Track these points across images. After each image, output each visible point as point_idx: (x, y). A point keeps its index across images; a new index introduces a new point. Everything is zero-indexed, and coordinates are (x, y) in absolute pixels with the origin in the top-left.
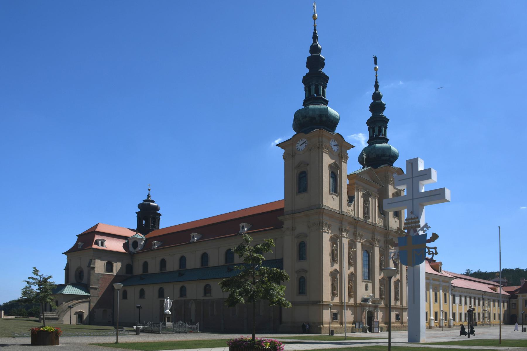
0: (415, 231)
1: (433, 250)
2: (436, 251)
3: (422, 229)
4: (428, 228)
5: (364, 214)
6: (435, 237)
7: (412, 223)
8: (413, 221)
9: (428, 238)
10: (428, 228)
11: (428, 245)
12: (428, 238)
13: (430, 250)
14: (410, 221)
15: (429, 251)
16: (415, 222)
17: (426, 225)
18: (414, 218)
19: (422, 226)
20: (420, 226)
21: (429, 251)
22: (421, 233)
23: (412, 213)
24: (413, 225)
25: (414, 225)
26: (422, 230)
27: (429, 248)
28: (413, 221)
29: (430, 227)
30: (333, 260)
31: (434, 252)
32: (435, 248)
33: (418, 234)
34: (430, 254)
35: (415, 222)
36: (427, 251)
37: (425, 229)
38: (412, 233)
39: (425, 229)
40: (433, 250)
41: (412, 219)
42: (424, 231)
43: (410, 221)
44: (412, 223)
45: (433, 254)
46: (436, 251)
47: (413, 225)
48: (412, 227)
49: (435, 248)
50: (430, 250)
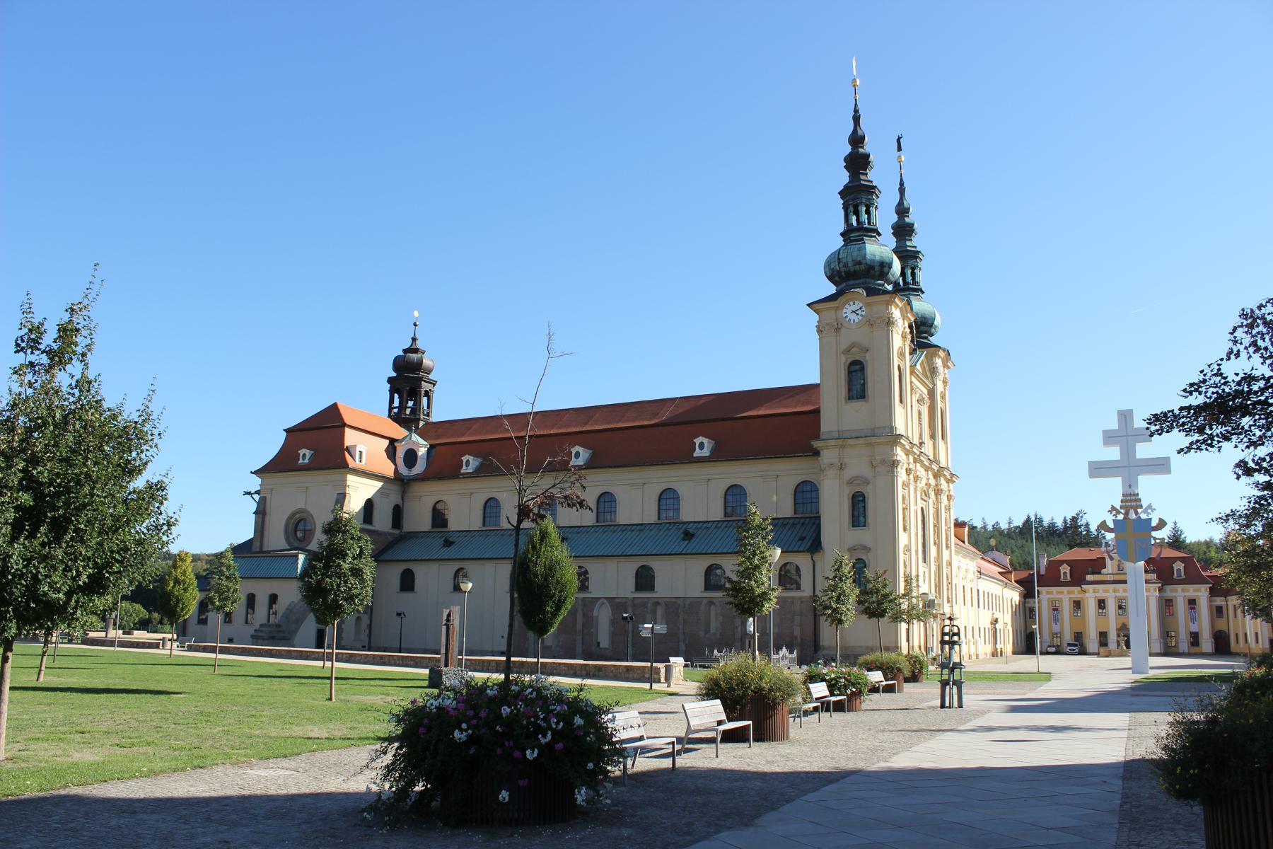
0: (1137, 513)
3: (1145, 511)
4: (1153, 510)
9: (1154, 524)
10: (1153, 510)
11: (1154, 534)
12: (1154, 524)
17: (1150, 506)
22: (1143, 516)
38: (1132, 516)
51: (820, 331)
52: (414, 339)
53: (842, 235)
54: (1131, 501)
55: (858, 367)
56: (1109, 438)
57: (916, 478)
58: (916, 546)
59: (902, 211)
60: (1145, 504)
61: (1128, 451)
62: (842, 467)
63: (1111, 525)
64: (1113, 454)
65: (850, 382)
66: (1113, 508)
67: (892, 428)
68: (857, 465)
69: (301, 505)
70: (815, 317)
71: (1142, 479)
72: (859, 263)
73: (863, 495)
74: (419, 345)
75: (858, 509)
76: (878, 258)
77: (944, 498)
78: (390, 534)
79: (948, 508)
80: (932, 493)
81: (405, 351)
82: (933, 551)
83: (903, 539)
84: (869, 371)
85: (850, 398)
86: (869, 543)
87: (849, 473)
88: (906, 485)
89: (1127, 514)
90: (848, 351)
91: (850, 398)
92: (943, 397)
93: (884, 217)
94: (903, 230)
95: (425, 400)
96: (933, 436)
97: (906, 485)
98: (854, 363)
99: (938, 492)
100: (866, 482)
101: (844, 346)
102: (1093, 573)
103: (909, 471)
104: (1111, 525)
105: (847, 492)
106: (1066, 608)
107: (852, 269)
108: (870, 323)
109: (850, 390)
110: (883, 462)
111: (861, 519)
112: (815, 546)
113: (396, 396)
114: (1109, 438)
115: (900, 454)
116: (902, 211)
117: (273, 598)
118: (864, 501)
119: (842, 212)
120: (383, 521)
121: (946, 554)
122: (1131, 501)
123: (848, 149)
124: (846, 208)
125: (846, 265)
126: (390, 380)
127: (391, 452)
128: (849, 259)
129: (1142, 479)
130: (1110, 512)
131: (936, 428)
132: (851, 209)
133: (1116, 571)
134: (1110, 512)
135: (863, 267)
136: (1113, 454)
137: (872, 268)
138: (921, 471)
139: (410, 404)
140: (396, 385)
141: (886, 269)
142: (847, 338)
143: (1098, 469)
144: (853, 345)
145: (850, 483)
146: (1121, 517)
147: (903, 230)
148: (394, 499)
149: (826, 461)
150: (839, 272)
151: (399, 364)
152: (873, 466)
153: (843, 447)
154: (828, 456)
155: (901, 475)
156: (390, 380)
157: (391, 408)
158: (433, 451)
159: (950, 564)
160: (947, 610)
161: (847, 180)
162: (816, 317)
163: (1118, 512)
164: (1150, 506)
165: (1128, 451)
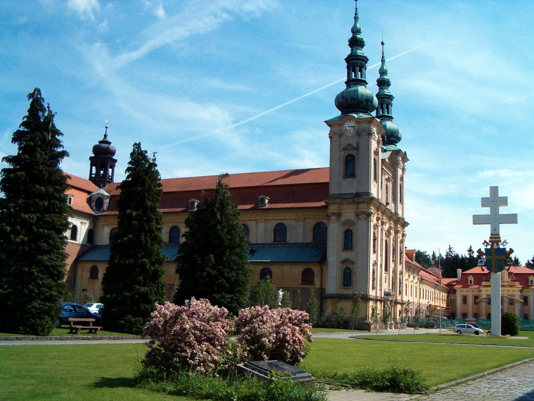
0: (498, 245)
4: (507, 243)
7: (495, 238)
10: (507, 243)
14: (494, 236)
17: (505, 241)
18: (497, 234)
19: (502, 241)
20: (500, 242)
22: (501, 247)
23: (495, 230)
37: (505, 244)
41: (495, 235)
43: (494, 236)
44: (495, 238)
48: (495, 242)
51: (331, 137)
52: (105, 136)
53: (346, 83)
54: (495, 238)
55: (351, 158)
56: (485, 202)
57: (383, 223)
58: (381, 261)
59: (383, 72)
60: (502, 240)
61: (495, 210)
62: (339, 215)
64: (486, 211)
66: (485, 242)
67: (368, 193)
70: (329, 129)
71: (502, 226)
72: (354, 99)
73: (351, 231)
74: (109, 139)
75: (348, 240)
76: (365, 97)
77: (400, 235)
79: (402, 242)
80: (392, 232)
81: (100, 142)
82: (392, 265)
83: (373, 257)
86: (352, 259)
88: (376, 227)
89: (492, 245)
90: (345, 149)
92: (402, 179)
93: (371, 74)
94: (383, 83)
95: (110, 170)
96: (394, 200)
97: (376, 227)
98: (349, 155)
99: (396, 232)
100: (353, 224)
101: (343, 147)
102: (486, 281)
103: (378, 219)
105: (342, 229)
106: (470, 300)
107: (350, 102)
110: (363, 213)
111: (350, 245)
112: (323, 260)
113: (94, 168)
114: (485, 202)
115: (373, 209)
116: (383, 72)
118: (351, 234)
119: (346, 70)
121: (399, 268)
122: (495, 238)
123: (350, 35)
124: (348, 68)
125: (346, 100)
126: (91, 158)
127: (89, 201)
128: (349, 97)
129: (502, 226)
130: (484, 244)
131: (397, 194)
132: (351, 68)
134: (484, 244)
135: (356, 101)
136: (486, 211)
137: (361, 102)
138: (385, 220)
139: (102, 172)
140: (94, 161)
141: (369, 103)
142: (345, 142)
143: (478, 220)
144: (349, 145)
145: (344, 223)
146: (489, 247)
147: (383, 83)
150: (343, 103)
151: (96, 149)
153: (340, 204)
154: (333, 208)
155: (374, 220)
156: (91, 158)
157: (91, 174)
158: (112, 200)
159: (401, 273)
160: (399, 298)
161: (350, 52)
163: (488, 244)
164: (505, 241)
165: (495, 210)
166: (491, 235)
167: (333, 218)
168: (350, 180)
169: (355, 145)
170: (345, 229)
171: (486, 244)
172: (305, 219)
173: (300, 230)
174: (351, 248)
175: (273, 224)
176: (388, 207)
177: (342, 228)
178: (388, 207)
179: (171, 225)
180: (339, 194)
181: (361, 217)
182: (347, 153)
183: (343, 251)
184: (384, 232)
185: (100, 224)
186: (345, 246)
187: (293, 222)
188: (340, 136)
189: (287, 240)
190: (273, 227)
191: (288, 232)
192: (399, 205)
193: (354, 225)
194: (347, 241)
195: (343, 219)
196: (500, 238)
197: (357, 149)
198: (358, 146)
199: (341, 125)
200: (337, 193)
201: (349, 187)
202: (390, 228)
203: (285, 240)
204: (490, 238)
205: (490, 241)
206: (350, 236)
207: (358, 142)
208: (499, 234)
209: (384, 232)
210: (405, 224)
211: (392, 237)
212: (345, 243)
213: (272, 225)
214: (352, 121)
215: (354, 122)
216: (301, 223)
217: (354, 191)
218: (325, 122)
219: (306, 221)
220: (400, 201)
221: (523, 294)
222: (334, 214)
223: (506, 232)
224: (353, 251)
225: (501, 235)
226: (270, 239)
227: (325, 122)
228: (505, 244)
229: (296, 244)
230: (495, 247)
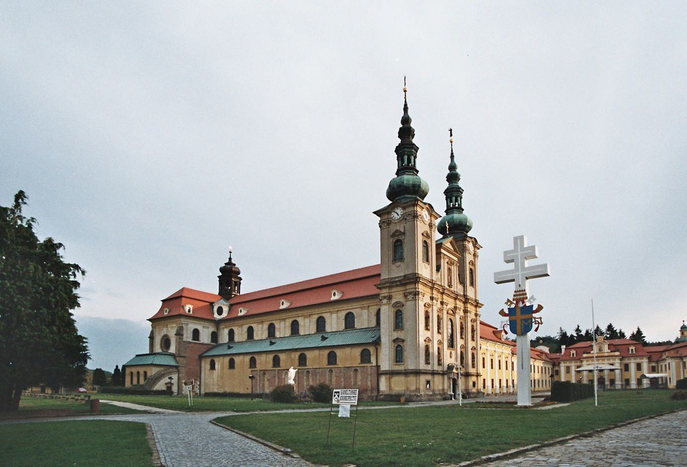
0: (523, 302)
1: (539, 320)
2: (541, 320)
4: (534, 300)
5: (448, 283)
6: (540, 308)
7: (520, 295)
8: (521, 293)
9: (534, 309)
10: (534, 300)
11: (534, 315)
12: (534, 309)
13: (536, 320)
14: (518, 293)
15: (535, 321)
16: (523, 294)
17: (532, 297)
18: (522, 291)
20: (527, 298)
21: (535, 321)
22: (528, 304)
24: (521, 297)
25: (522, 296)
26: (528, 301)
27: (535, 318)
28: (521, 293)
29: (535, 299)
30: (427, 327)
31: (540, 322)
32: (541, 318)
33: (525, 305)
34: (536, 324)
35: (523, 294)
36: (533, 320)
39: (532, 300)
40: (539, 320)
41: (520, 291)
42: (531, 302)
43: (518, 293)
44: (520, 295)
45: (539, 323)
46: (541, 320)
47: (521, 297)
48: (520, 299)
49: (541, 318)
50: (536, 320)
51: (380, 227)
54: (520, 295)
55: (399, 243)
60: (528, 296)
63: (507, 312)
65: (395, 251)
66: (508, 300)
68: (398, 297)
69: (165, 333)
73: (401, 311)
78: (210, 344)
84: (404, 245)
85: (395, 260)
87: (393, 301)
89: (517, 303)
90: (393, 236)
91: (395, 260)
96: (462, 282)
99: (466, 311)
102: (587, 353)
104: (507, 312)
105: (393, 310)
108: (404, 218)
109: (395, 256)
110: (410, 293)
111: (400, 324)
115: (421, 288)
117: (145, 373)
120: (205, 338)
122: (520, 295)
130: (506, 303)
133: (598, 352)
134: (506, 303)
142: (393, 228)
144: (397, 231)
146: (513, 306)
148: (212, 329)
149: (383, 295)
152: (406, 296)
162: (379, 219)
163: (512, 303)
166: (515, 292)
167: (385, 301)
168: (399, 263)
169: (402, 230)
170: (395, 310)
171: (509, 303)
172: (369, 306)
173: (365, 317)
174: (402, 328)
175: (344, 313)
176: (452, 289)
177: (393, 310)
178: (452, 289)
179: (269, 323)
180: (389, 278)
181: (408, 297)
182: (396, 238)
183: (394, 331)
184: (445, 312)
185: (221, 327)
186: (396, 326)
187: (358, 310)
188: (389, 224)
189: (356, 327)
190: (344, 316)
191: (356, 319)
192: (469, 288)
193: (403, 305)
194: (398, 321)
195: (393, 301)
196: (526, 294)
197: (404, 233)
198: (404, 230)
199: (389, 213)
200: (387, 277)
201: (398, 271)
202: (455, 308)
203: (354, 327)
204: (514, 296)
205: (513, 300)
206: (401, 317)
207: (404, 227)
208: (525, 290)
209: (445, 312)
210: (477, 305)
211: (458, 317)
212: (396, 323)
213: (343, 314)
214: (399, 208)
215: (401, 209)
216: (366, 311)
217: (402, 274)
218: (374, 213)
219: (370, 307)
220: (472, 284)
221: (622, 362)
222: (385, 297)
223: (530, 287)
224: (403, 330)
225: (527, 291)
226: (342, 327)
227: (374, 213)
228: (532, 300)
229: (362, 329)
230: (521, 305)
